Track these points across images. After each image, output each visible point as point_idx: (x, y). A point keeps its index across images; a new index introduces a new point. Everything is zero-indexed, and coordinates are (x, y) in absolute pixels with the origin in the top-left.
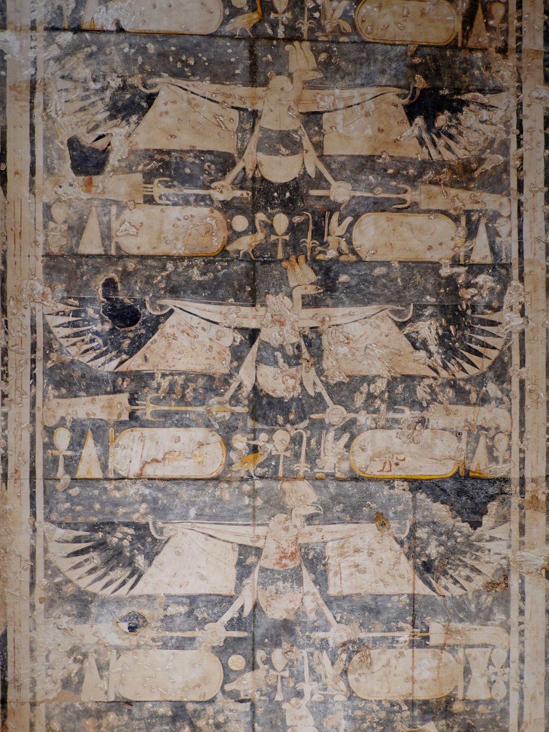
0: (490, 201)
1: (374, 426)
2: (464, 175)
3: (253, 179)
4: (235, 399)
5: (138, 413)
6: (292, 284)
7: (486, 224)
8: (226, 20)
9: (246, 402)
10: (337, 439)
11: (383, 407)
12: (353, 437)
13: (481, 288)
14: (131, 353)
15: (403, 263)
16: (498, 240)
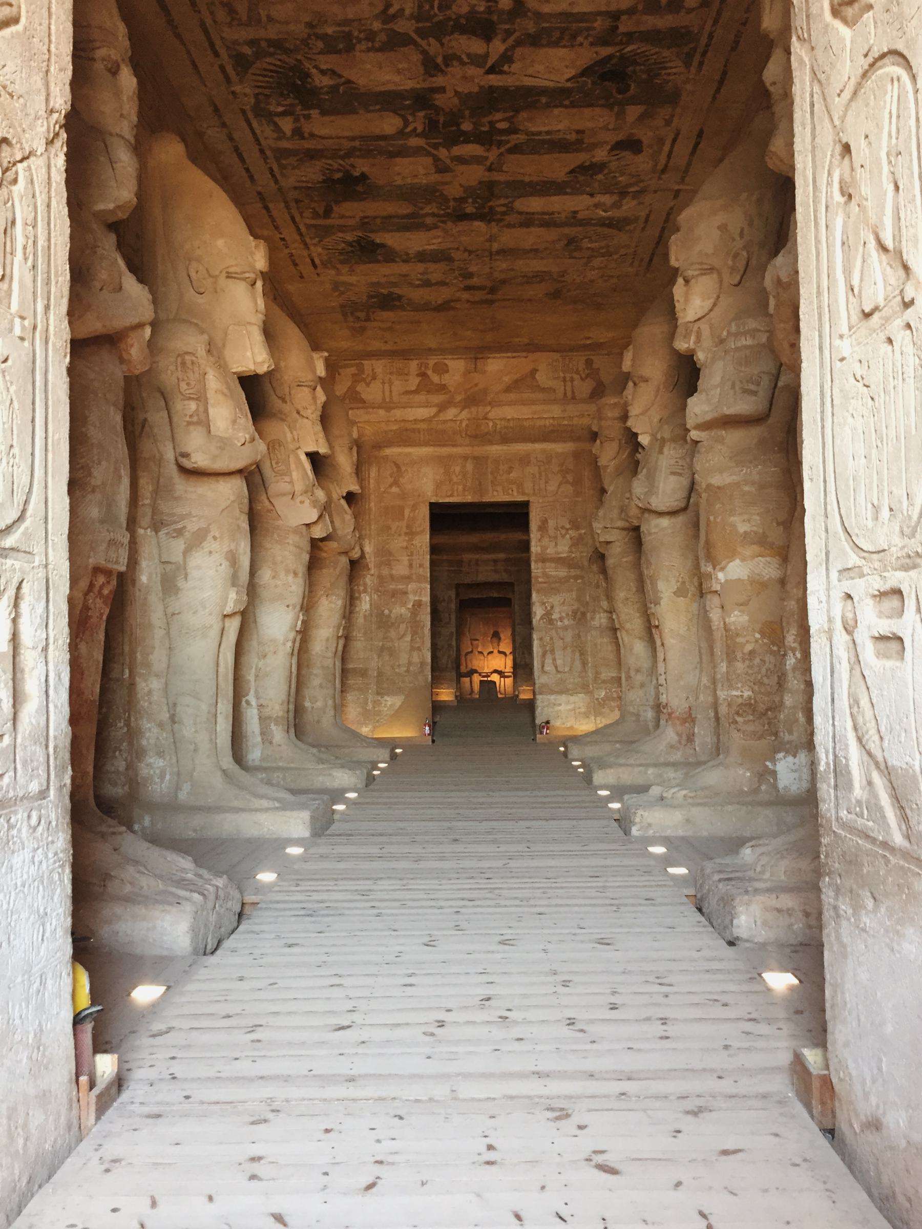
0: (285, 144)
1: (363, 22)
2: (312, 155)
3: (491, 145)
4: (508, 33)
5: (610, 20)
6: (456, 98)
7: (284, 134)
8: (512, 202)
9: (498, 31)
10: (402, 10)
11: (356, 34)
12: (384, 11)
13: (279, 104)
14: (609, 57)
15: (353, 112)
16: (272, 128)
